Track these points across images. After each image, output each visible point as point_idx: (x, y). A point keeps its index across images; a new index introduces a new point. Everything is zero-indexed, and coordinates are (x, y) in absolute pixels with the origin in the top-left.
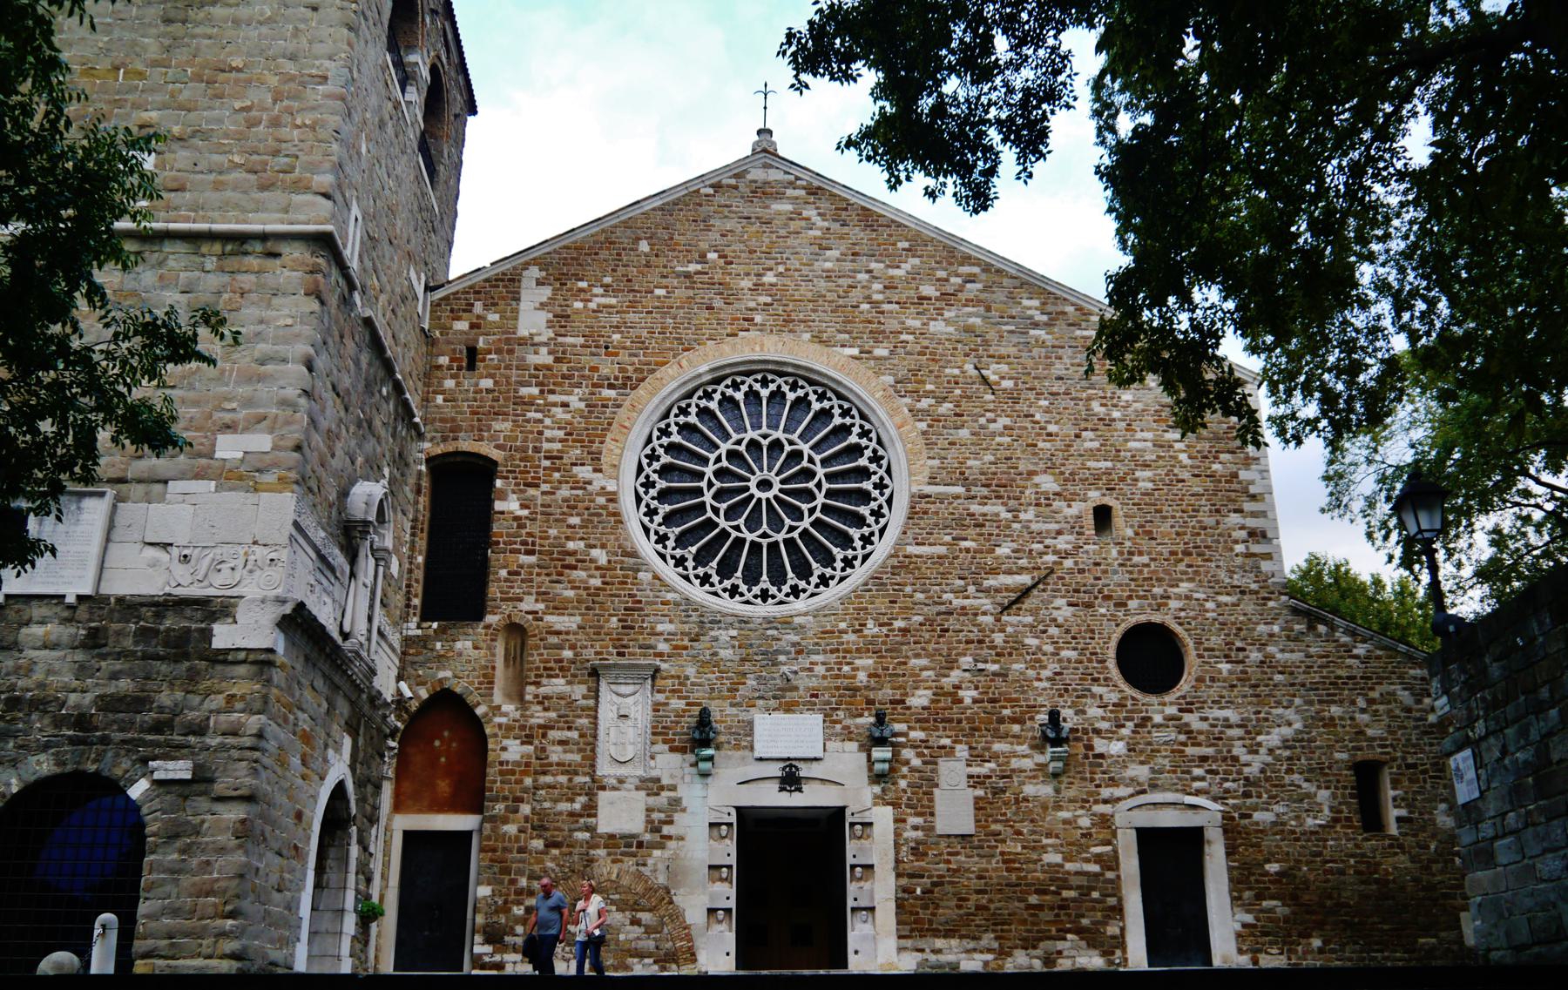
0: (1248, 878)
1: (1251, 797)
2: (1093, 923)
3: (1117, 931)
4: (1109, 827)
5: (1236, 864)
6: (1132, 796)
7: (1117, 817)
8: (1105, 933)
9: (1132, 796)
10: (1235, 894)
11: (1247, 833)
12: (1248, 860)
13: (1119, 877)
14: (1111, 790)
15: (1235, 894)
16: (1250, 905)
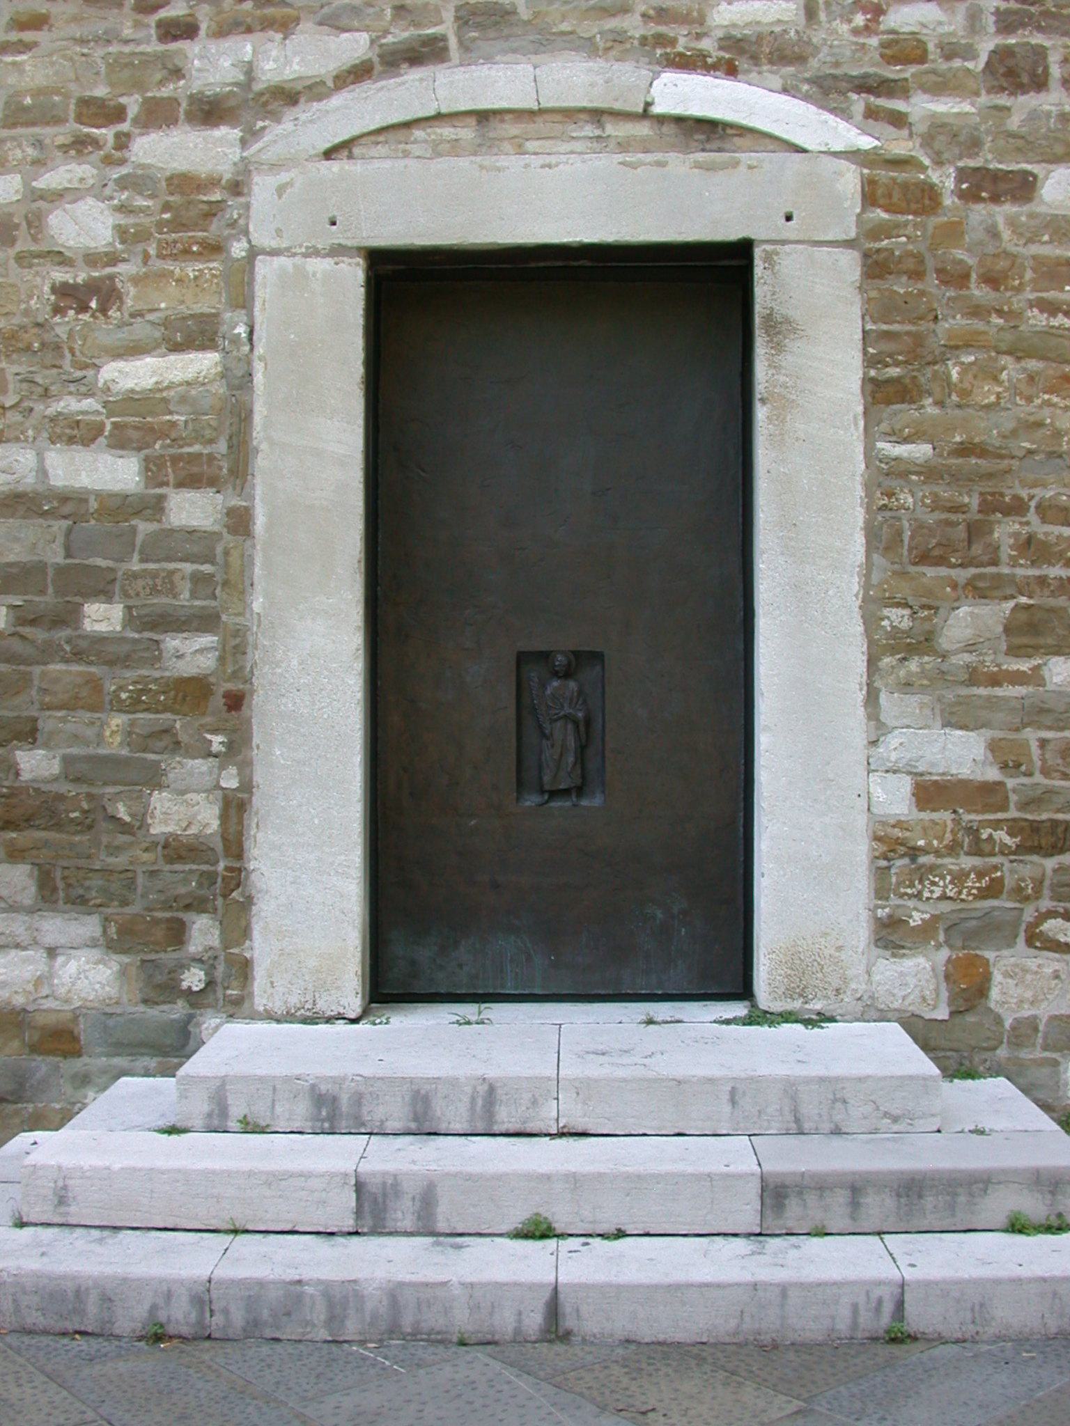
0: (976, 531)
1: (1039, 83)
2: (74, 771)
3: (208, 818)
4: (215, 249)
5: (920, 451)
6: (359, 73)
7: (262, 188)
8: (135, 828)
9: (359, 73)
10: (897, 617)
11: (992, 280)
12: (989, 431)
13: (240, 522)
14: (246, 48)
15: (897, 617)
16: (974, 677)
